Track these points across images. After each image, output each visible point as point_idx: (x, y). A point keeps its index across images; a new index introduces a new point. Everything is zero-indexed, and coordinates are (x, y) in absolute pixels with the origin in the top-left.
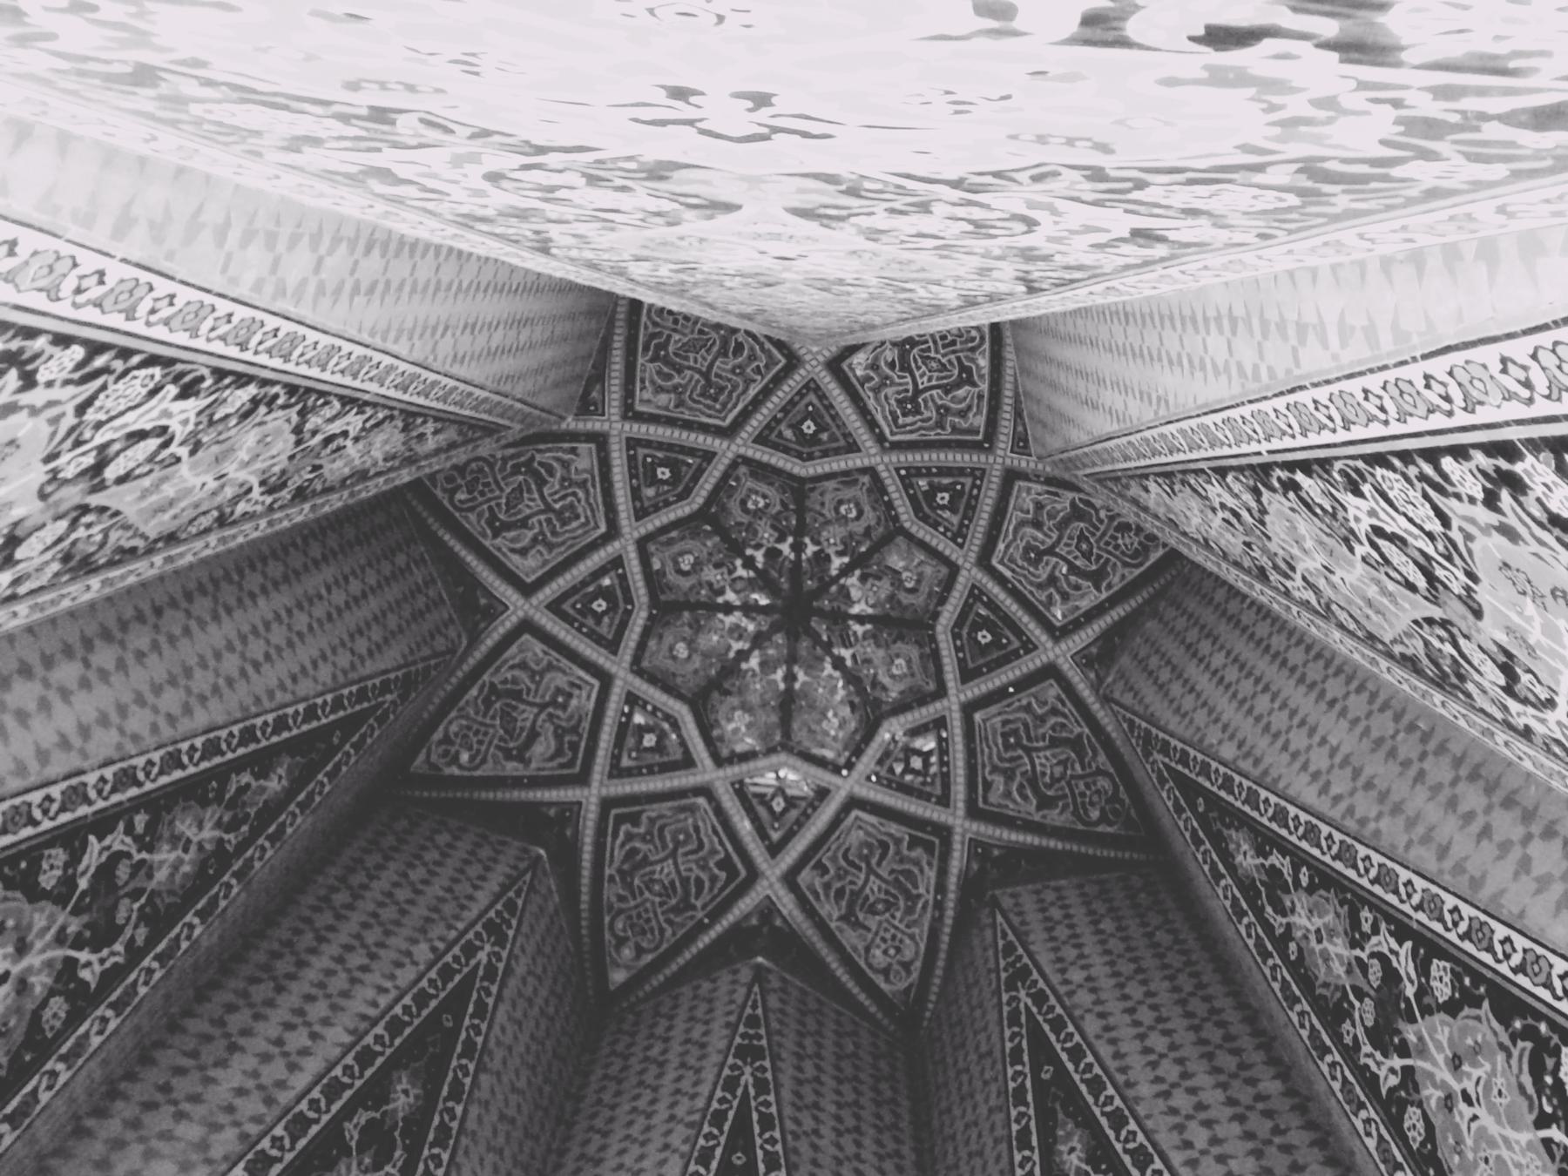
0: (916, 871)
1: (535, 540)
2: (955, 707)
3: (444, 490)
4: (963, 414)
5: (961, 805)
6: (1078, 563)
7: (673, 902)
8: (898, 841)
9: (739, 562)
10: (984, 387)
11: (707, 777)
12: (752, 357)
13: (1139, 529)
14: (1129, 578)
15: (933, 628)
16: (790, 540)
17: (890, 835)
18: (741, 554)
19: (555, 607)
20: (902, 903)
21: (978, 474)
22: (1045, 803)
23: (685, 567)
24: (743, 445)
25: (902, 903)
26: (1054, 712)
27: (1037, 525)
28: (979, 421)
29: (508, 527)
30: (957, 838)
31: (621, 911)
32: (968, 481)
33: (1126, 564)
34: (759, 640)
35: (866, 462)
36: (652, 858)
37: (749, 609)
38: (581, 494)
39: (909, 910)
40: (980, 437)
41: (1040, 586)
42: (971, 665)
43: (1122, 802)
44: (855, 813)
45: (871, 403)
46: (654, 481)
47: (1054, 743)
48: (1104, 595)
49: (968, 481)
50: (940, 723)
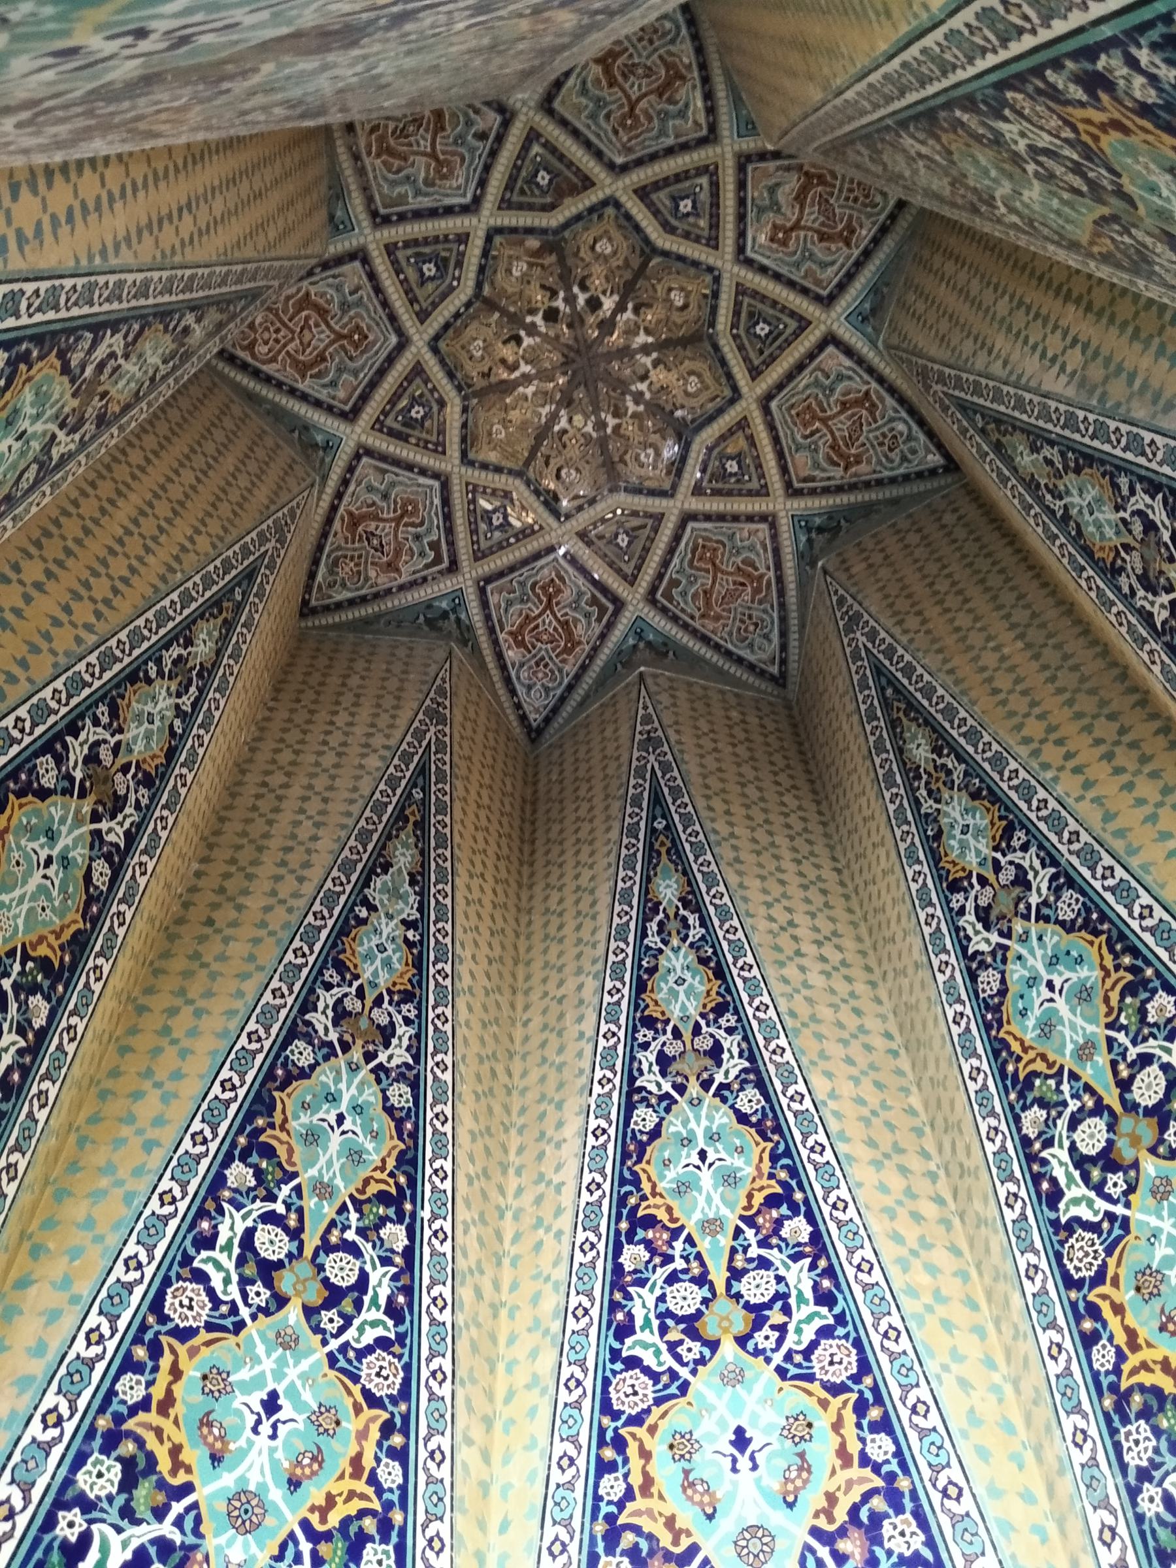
0: (391, 176)
1: (832, 390)
2: (416, 338)
3: (916, 439)
4: (509, 603)
5: (375, 253)
6: (373, 525)
7: (619, 62)
8: (418, 193)
9: (648, 396)
10: (502, 636)
11: (620, 184)
12: (684, 594)
13: (344, 585)
14: (331, 539)
15: (465, 398)
16: (609, 430)
17: (427, 195)
18: (647, 404)
19: (804, 323)
20: (392, 142)
21: (479, 556)
22: (306, 301)
23: (693, 379)
24: (672, 508)
25: (392, 142)
26: (333, 384)
27: (417, 537)
28: (493, 599)
29: (858, 403)
30: (365, 224)
31: (673, 41)
32: (484, 545)
33: (339, 548)
34: (607, 326)
35: (568, 525)
36: (652, 97)
37: (625, 353)
38: (798, 437)
39: (382, 139)
40: (489, 588)
41: (393, 484)
42: (418, 381)
43: (243, 348)
44: (468, 199)
45: (581, 581)
46: (739, 457)
47: (321, 358)
48: (341, 510)
49: (484, 545)
50: (423, 316)
